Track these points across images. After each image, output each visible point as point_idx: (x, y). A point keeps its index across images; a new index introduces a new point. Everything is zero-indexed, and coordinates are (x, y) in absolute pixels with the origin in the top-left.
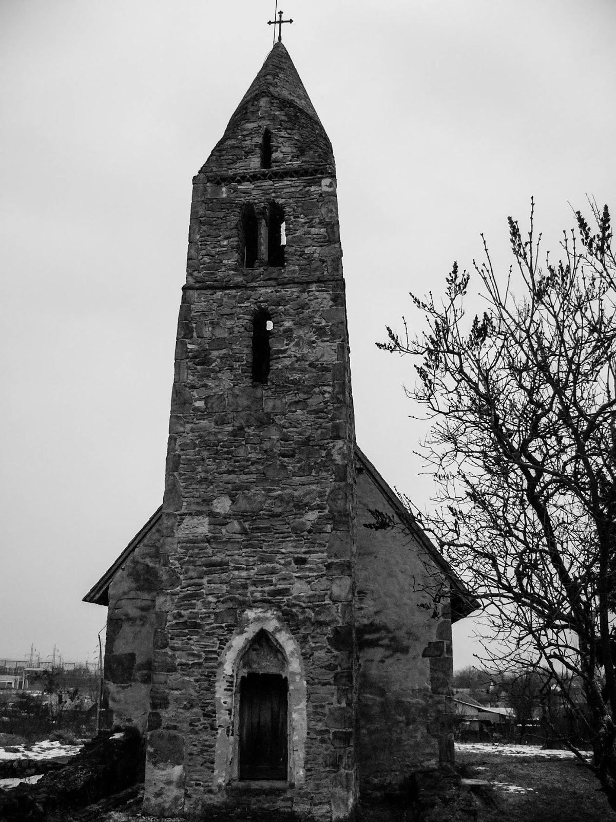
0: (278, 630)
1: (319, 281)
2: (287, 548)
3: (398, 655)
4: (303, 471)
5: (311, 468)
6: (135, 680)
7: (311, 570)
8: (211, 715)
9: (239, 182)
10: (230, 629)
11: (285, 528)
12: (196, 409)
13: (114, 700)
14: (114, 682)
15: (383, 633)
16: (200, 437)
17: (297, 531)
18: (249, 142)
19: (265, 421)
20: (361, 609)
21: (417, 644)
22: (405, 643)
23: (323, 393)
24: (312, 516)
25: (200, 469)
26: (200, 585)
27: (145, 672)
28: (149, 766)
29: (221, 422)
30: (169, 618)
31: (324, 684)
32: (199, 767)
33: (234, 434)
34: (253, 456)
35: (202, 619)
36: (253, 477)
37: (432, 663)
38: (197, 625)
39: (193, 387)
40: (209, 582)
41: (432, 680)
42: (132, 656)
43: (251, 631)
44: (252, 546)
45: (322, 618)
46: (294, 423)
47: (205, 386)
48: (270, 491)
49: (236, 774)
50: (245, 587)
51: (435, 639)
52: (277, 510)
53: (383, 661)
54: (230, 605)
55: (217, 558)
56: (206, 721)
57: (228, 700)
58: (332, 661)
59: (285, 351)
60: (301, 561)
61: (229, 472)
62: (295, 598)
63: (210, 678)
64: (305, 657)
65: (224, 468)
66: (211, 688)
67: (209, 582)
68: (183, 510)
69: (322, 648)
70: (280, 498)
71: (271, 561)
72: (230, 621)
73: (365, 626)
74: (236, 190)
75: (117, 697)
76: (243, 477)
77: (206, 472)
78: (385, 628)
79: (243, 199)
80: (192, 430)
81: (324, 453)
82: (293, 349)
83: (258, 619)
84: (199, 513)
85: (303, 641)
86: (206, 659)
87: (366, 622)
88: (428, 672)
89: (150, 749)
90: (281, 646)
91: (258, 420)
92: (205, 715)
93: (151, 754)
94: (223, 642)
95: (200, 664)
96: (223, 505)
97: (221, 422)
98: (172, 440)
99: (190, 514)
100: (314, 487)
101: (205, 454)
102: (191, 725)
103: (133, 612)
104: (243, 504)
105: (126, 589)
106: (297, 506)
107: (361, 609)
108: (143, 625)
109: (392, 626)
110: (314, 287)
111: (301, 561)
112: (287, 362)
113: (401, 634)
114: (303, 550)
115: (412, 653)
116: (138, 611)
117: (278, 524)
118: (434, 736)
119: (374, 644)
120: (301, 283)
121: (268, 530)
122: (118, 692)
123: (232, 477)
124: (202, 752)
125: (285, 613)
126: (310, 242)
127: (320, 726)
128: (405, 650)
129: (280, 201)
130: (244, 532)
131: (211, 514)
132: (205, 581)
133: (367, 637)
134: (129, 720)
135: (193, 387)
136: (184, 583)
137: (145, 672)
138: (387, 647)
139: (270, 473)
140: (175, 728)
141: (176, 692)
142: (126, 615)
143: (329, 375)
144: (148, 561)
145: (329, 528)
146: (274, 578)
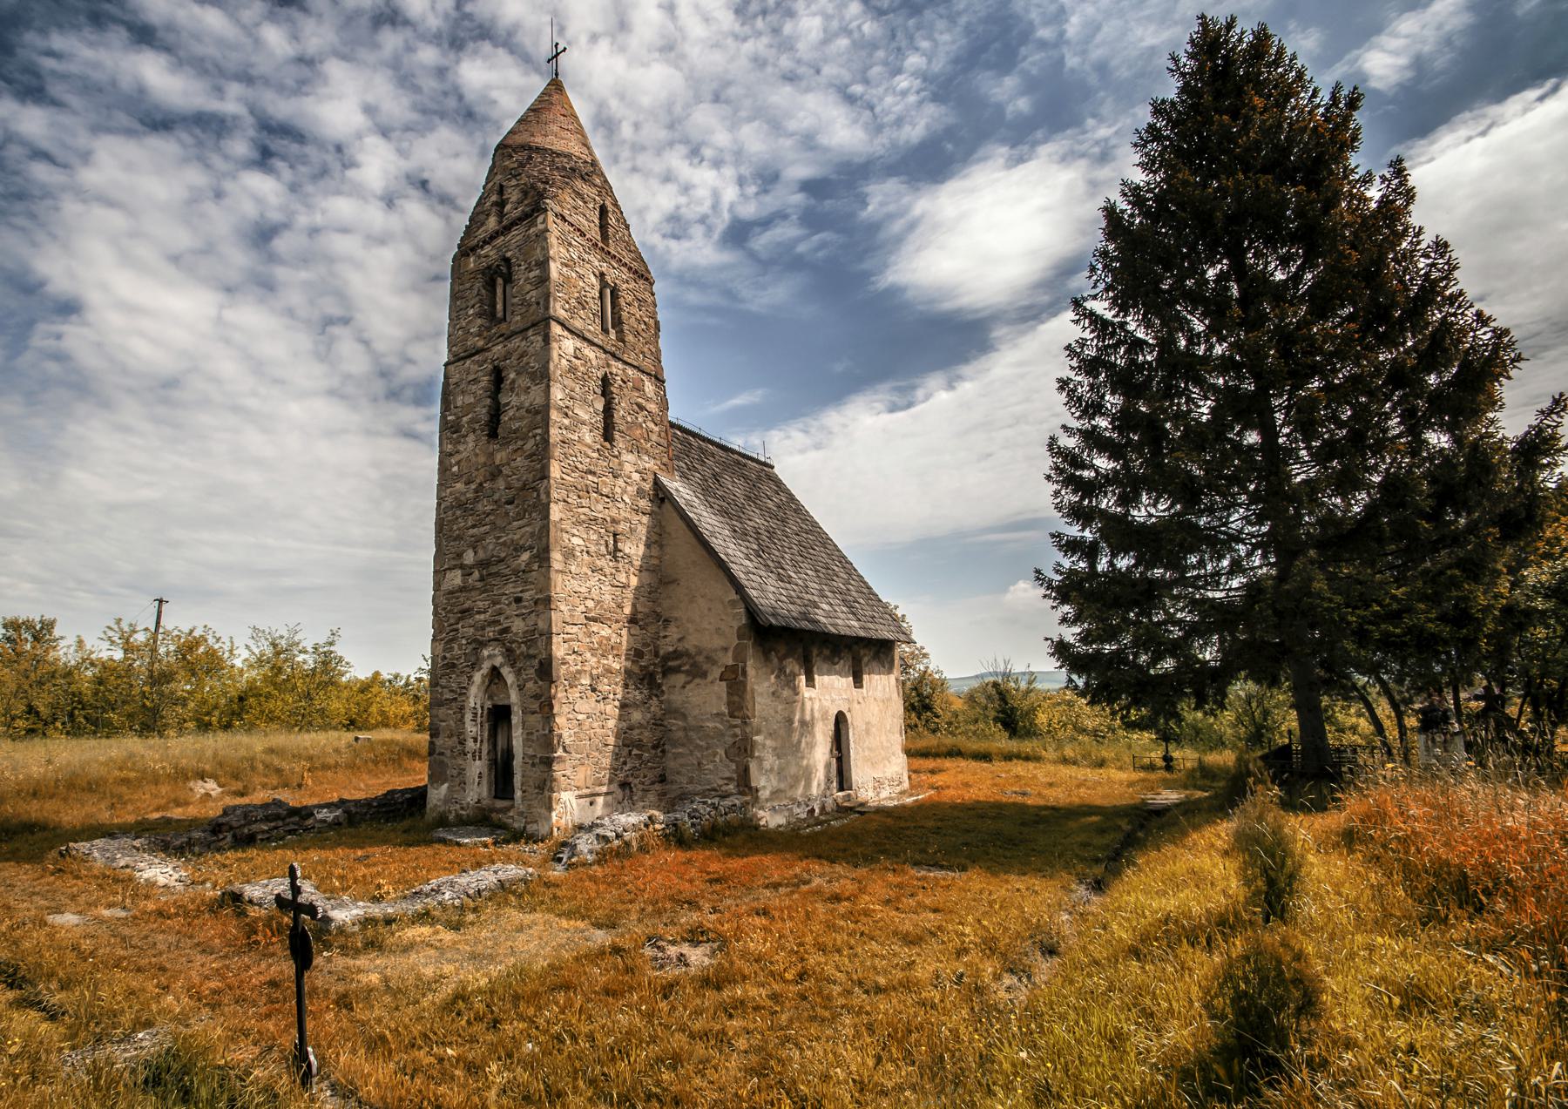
0: (502, 665)
1: (533, 325)
2: (509, 589)
3: (697, 681)
4: (519, 517)
5: (525, 511)
7: (525, 607)
8: (462, 742)
9: (482, 247)
11: (507, 571)
12: (453, 474)
15: (685, 659)
16: (456, 498)
17: (516, 572)
19: (495, 474)
20: (665, 637)
21: (714, 668)
22: (705, 667)
23: (535, 436)
24: (525, 556)
25: (455, 527)
26: (457, 630)
29: (468, 483)
31: (533, 713)
33: (476, 491)
34: (488, 508)
37: (729, 687)
38: (454, 666)
40: (463, 627)
41: (729, 704)
43: (486, 666)
45: (532, 652)
47: (458, 452)
48: (499, 538)
49: (485, 793)
50: (483, 628)
51: (730, 662)
52: (503, 555)
53: (684, 687)
54: (474, 645)
57: (474, 729)
58: (538, 691)
59: (508, 404)
60: (518, 600)
61: (474, 526)
63: (462, 708)
64: (521, 688)
66: (461, 720)
67: (463, 627)
69: (531, 679)
70: (504, 544)
71: (499, 603)
73: (669, 653)
74: (479, 257)
76: (482, 529)
78: (687, 654)
80: (451, 494)
81: (535, 494)
83: (490, 657)
85: (518, 673)
87: (671, 649)
88: (724, 695)
92: (460, 743)
94: (470, 678)
95: (455, 699)
97: (468, 483)
98: (439, 504)
99: (449, 569)
100: (527, 529)
104: (481, 555)
106: (515, 550)
107: (665, 637)
109: (693, 651)
110: (530, 332)
111: (518, 600)
112: (511, 413)
113: (700, 659)
115: (710, 678)
117: (501, 567)
118: (731, 761)
119: (677, 670)
120: (522, 331)
121: (497, 574)
123: (475, 530)
124: (459, 774)
126: (528, 287)
127: (530, 752)
128: (704, 675)
129: (509, 254)
130: (482, 579)
131: (462, 567)
133: (670, 664)
136: (448, 629)
138: (688, 673)
139: (499, 522)
143: (539, 417)
145: (535, 567)
146: (502, 618)
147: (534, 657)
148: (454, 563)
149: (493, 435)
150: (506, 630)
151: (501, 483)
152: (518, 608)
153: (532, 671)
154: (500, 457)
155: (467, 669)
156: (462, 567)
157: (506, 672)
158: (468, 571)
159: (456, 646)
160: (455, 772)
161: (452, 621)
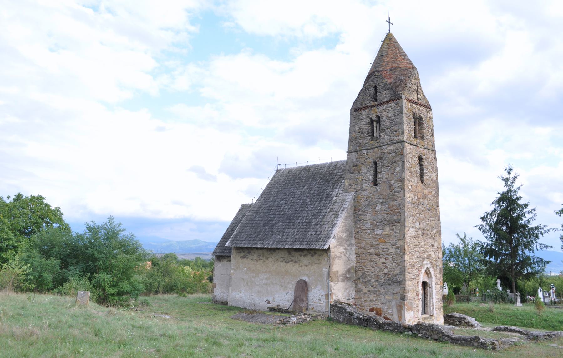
0: (430, 268)
6: (339, 281)
7: (435, 249)
10: (421, 267)
13: (334, 289)
14: (333, 282)
18: (413, 87)
24: (435, 231)
27: (342, 278)
28: (406, 312)
30: (408, 263)
32: (416, 312)
35: (415, 263)
36: (422, 216)
39: (409, 181)
42: (338, 271)
43: (425, 267)
44: (424, 240)
46: (429, 199)
52: (428, 228)
54: (420, 259)
55: (417, 243)
56: (417, 297)
59: (426, 173)
60: (433, 246)
61: (418, 213)
62: (432, 257)
64: (436, 276)
65: (417, 212)
68: (409, 226)
72: (421, 264)
75: (334, 288)
77: (413, 212)
79: (414, 110)
82: (429, 173)
83: (426, 264)
84: (412, 227)
85: (435, 272)
86: (417, 277)
89: (406, 307)
90: (430, 273)
91: (423, 197)
93: (407, 309)
94: (420, 271)
95: (415, 278)
96: (417, 225)
100: (434, 222)
101: (413, 206)
102: (414, 298)
103: (338, 254)
104: (422, 226)
105: (335, 245)
108: (340, 260)
110: (430, 151)
114: (433, 242)
116: (340, 254)
122: (334, 286)
123: (418, 215)
124: (417, 306)
125: (431, 263)
127: (438, 297)
131: (416, 228)
132: (414, 250)
134: (337, 297)
135: (409, 181)
136: (410, 251)
137: (342, 278)
139: (426, 216)
140: (411, 299)
141: (410, 288)
142: (336, 255)
144: (341, 234)
145: (438, 236)
146: (427, 250)
147: (439, 266)
148: (412, 225)
149: (422, 181)
150: (430, 255)
151: (426, 202)
152: (433, 248)
153: (438, 271)
154: (426, 192)
155: (420, 268)
156: (416, 228)
157: (431, 270)
158: (417, 230)
159: (414, 258)
160: (415, 306)
161: (412, 248)
